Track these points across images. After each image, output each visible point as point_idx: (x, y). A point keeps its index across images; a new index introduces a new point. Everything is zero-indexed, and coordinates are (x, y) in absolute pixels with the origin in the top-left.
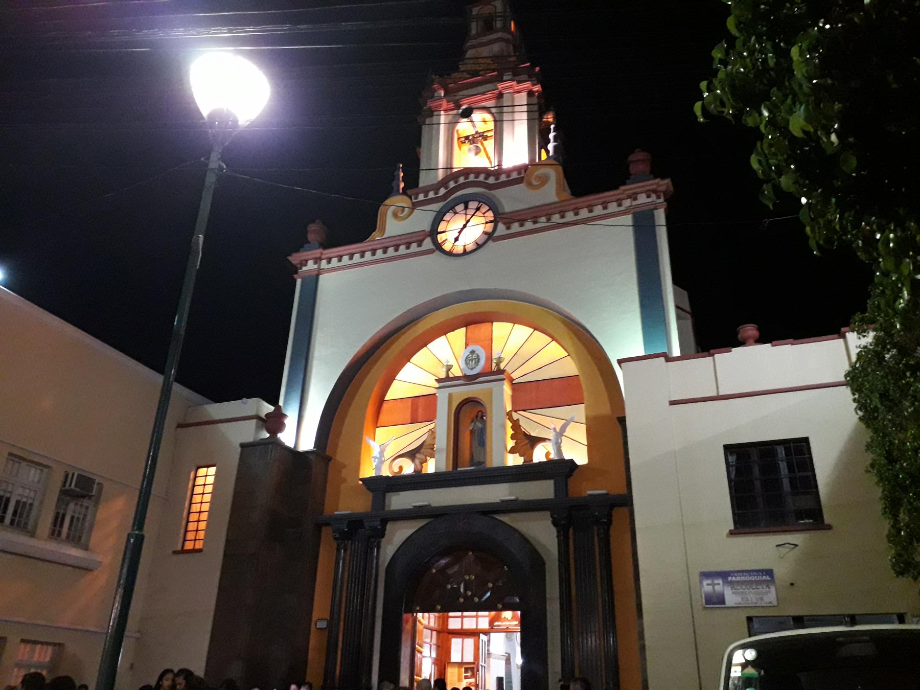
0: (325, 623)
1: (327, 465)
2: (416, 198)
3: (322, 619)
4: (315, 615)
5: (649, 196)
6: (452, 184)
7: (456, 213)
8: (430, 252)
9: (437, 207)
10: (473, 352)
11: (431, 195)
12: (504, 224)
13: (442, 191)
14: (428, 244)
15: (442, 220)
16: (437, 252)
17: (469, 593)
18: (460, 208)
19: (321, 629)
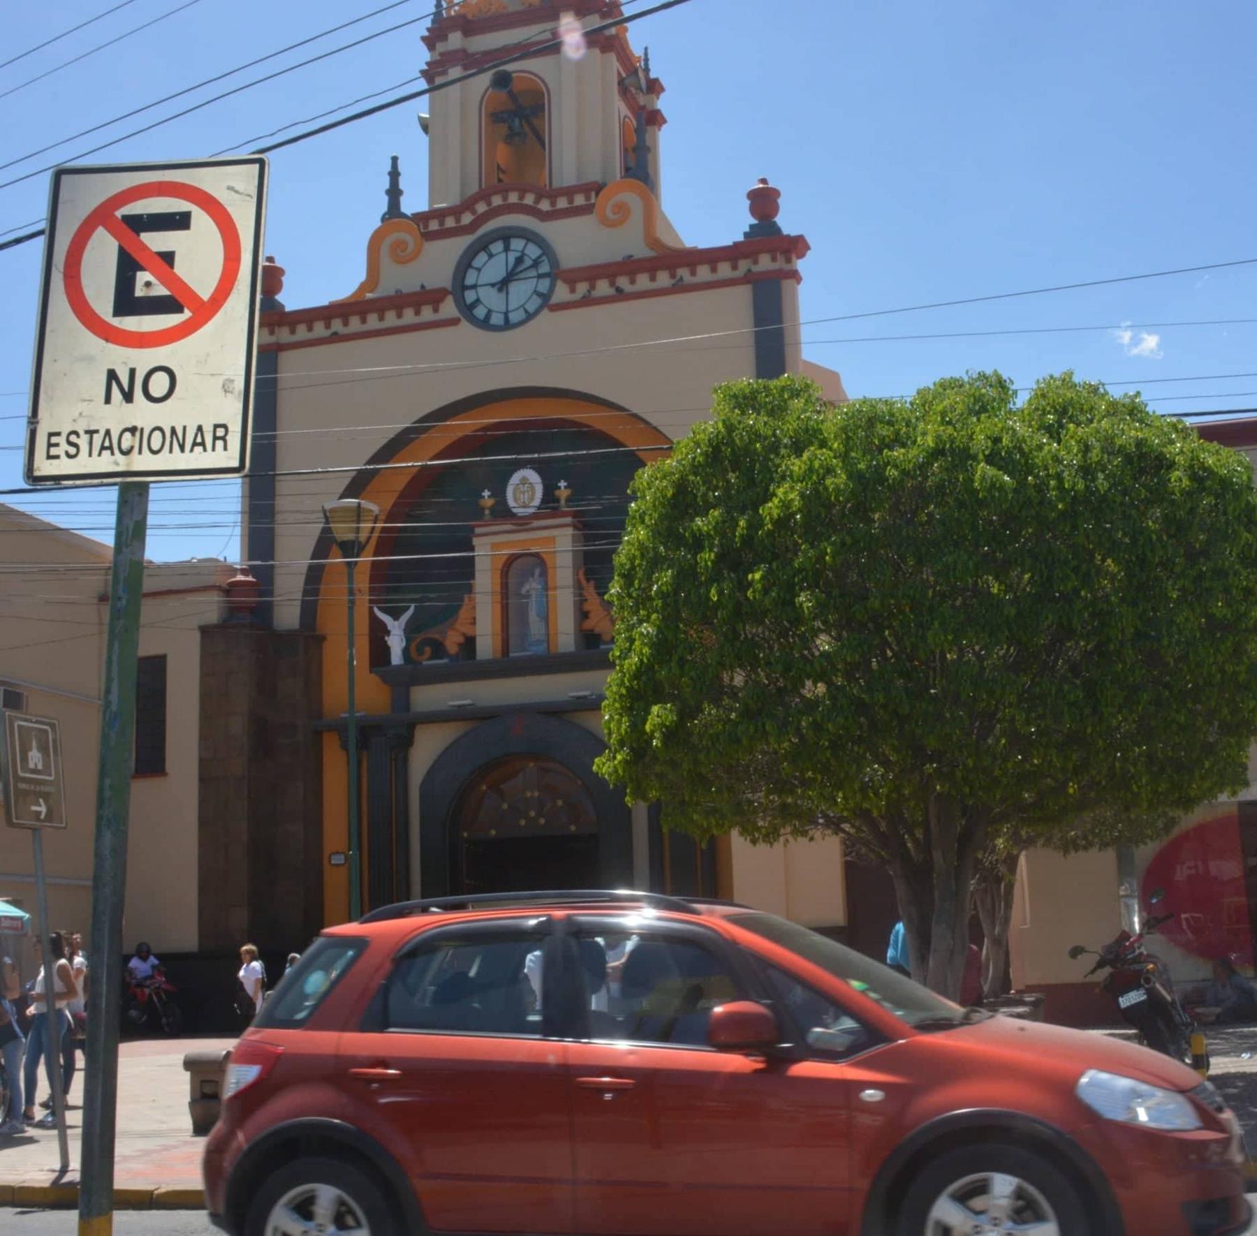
0: (342, 857)
1: (321, 648)
2: (426, 226)
3: (337, 853)
4: (328, 849)
5: (774, 259)
6: (481, 208)
7: (491, 256)
8: (454, 322)
9: (460, 244)
10: (524, 481)
11: (450, 222)
12: (565, 281)
13: (467, 219)
14: (449, 308)
15: (469, 266)
16: (464, 324)
17: (533, 814)
18: (497, 247)
19: (338, 865)
